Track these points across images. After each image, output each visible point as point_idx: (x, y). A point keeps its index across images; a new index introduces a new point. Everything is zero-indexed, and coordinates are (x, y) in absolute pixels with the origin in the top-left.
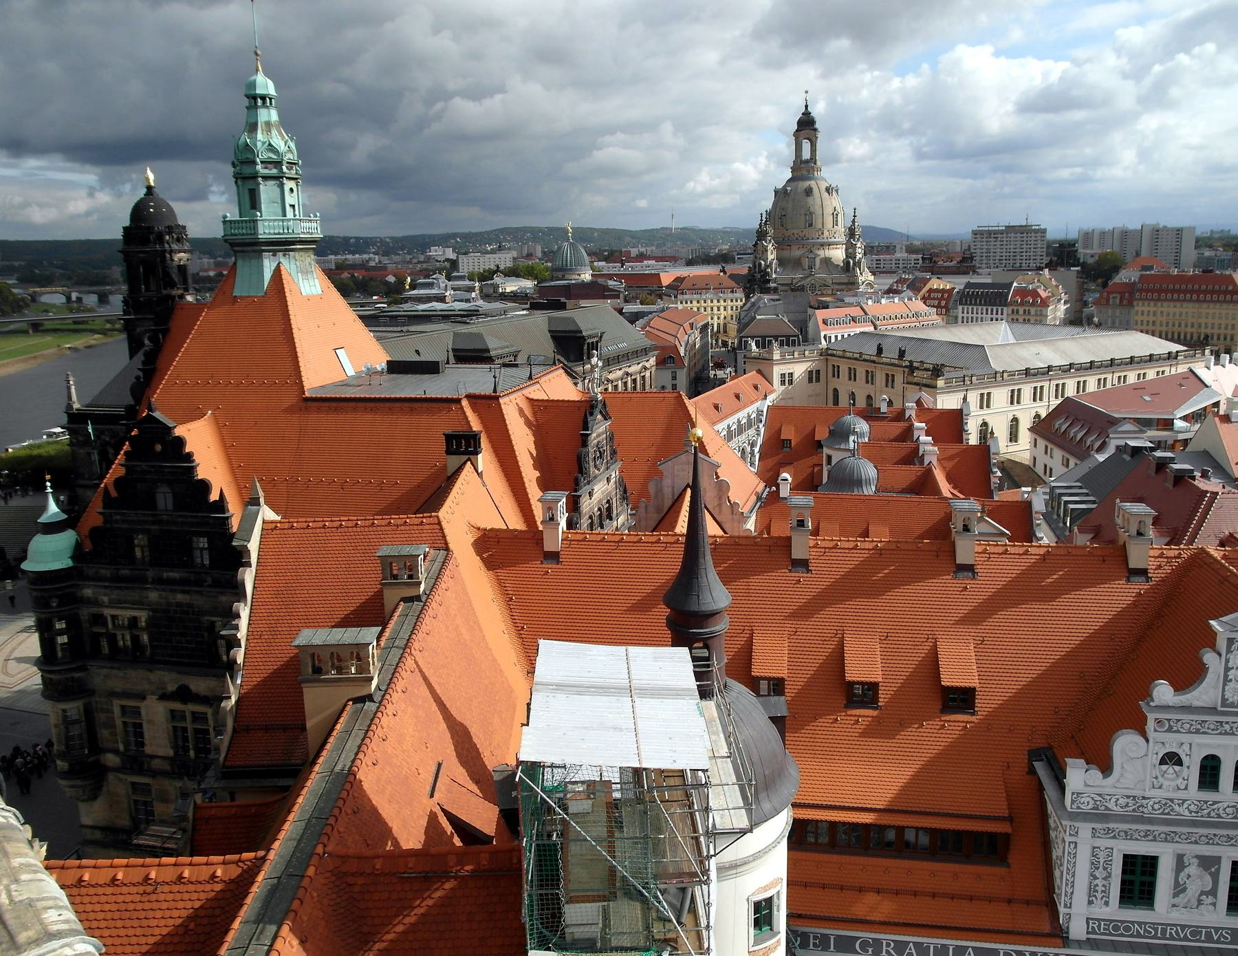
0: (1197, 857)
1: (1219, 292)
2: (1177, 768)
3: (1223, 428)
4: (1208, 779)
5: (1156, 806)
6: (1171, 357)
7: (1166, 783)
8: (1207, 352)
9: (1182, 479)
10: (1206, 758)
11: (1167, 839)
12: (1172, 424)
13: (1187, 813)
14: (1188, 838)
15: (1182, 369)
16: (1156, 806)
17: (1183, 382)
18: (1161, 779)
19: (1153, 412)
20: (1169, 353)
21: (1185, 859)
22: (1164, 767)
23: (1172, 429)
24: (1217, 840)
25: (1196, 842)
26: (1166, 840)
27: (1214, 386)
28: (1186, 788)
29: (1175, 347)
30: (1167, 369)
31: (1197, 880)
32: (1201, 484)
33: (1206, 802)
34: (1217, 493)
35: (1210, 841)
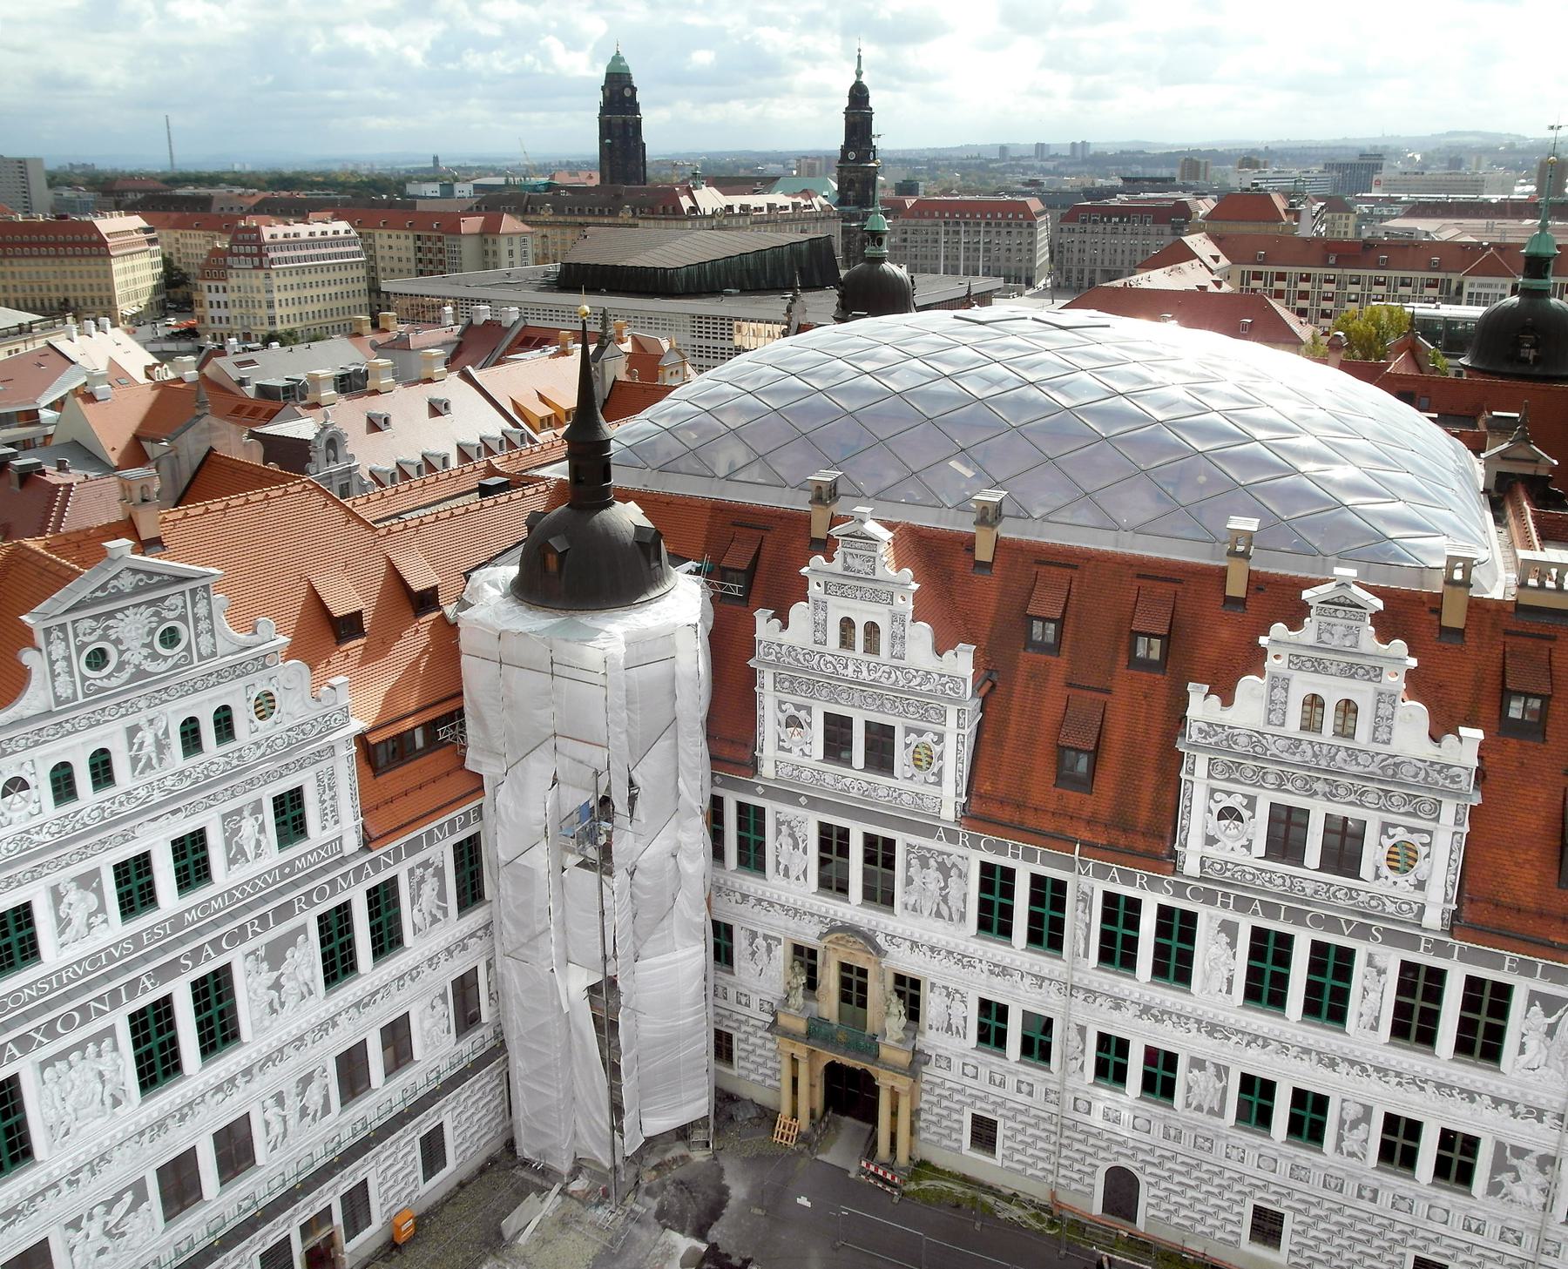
0: (73, 880)
1: (74, 244)
2: (23, 793)
3: (88, 409)
4: (64, 791)
5: (11, 847)
6: (22, 330)
7: (15, 816)
8: (69, 319)
9: (28, 476)
10: (55, 769)
11: (34, 875)
12: (38, 416)
13: (48, 838)
14: (59, 864)
15: (40, 344)
16: (11, 847)
17: (42, 360)
18: (8, 814)
19: (8, 405)
20: (20, 325)
21: (61, 888)
22: (9, 799)
23: (38, 423)
24: (90, 852)
25: (68, 865)
26: (33, 879)
27: (82, 361)
28: (40, 812)
29: (26, 317)
30: (21, 347)
31: (79, 903)
32: (53, 477)
33: (66, 816)
34: (71, 485)
35: (82, 856)
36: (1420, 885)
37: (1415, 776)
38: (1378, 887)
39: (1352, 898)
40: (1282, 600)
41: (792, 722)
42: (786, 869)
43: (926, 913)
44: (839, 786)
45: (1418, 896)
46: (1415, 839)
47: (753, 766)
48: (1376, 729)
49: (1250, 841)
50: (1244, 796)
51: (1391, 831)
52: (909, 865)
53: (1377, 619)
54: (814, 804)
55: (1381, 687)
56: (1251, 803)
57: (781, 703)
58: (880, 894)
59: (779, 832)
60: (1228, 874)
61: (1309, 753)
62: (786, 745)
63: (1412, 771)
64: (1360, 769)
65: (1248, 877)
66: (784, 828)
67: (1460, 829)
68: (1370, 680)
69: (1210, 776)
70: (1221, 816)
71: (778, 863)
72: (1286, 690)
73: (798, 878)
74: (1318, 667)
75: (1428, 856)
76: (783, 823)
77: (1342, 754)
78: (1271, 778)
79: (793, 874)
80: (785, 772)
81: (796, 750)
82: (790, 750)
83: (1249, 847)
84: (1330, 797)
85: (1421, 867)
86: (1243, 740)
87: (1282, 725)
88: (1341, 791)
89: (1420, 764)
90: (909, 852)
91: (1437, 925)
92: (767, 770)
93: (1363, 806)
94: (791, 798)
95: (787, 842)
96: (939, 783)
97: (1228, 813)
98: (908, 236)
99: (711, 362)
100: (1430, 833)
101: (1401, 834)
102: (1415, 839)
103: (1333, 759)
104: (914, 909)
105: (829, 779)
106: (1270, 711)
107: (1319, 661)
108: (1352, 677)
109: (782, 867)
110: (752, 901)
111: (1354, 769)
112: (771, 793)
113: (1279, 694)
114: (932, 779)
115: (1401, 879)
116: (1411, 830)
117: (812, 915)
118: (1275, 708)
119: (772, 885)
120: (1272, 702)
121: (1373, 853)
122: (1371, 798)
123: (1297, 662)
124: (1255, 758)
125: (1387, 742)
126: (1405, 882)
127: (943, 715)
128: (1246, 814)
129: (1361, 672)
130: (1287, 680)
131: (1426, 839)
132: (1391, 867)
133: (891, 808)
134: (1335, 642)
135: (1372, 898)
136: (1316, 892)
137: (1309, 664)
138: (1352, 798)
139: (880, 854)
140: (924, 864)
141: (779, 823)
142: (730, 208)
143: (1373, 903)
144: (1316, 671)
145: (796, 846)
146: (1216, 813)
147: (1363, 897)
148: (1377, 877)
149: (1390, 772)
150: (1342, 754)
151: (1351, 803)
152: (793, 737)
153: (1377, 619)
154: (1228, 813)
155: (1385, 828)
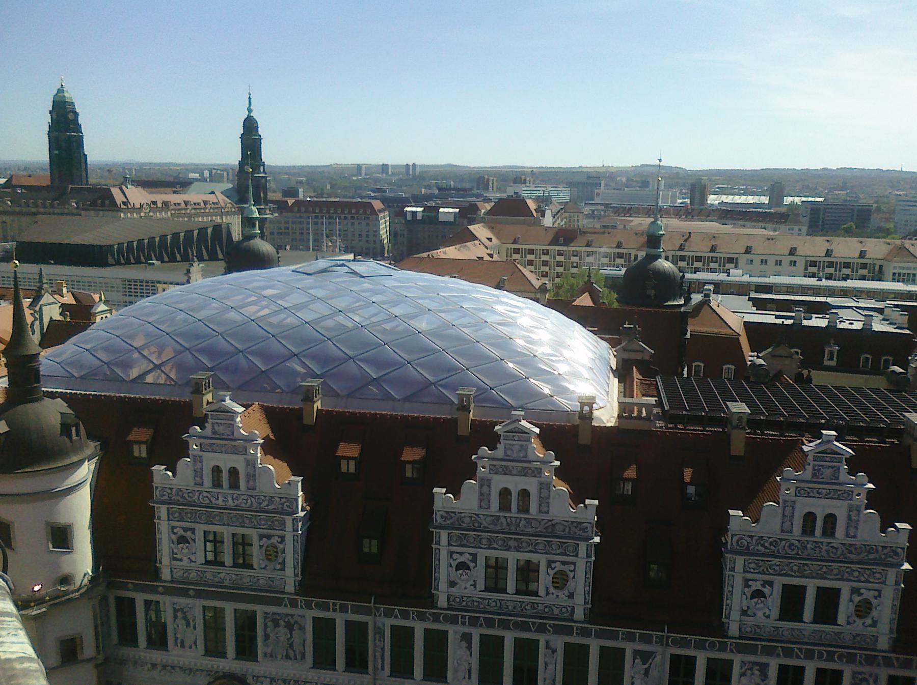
36: (571, 596)
38: (549, 600)
39: (535, 609)
40: (485, 434)
41: (182, 540)
42: (182, 642)
43: (279, 657)
45: (570, 603)
46: (566, 568)
47: (155, 574)
48: (540, 505)
49: (475, 581)
51: (553, 565)
52: (266, 626)
54: (199, 595)
56: (474, 557)
57: (173, 528)
58: (246, 650)
59: (175, 617)
60: (464, 603)
61: (505, 523)
62: (178, 556)
63: (562, 528)
64: (533, 530)
65: (476, 604)
66: (179, 614)
67: (589, 560)
68: (535, 476)
69: (449, 544)
71: (176, 639)
72: (489, 486)
73: (191, 647)
74: (506, 472)
75: (574, 577)
76: (179, 610)
77: (523, 522)
78: (484, 541)
79: (187, 644)
80: (178, 575)
81: (185, 559)
82: (181, 560)
83: (475, 586)
84: (518, 549)
85: (571, 584)
86: (467, 520)
87: (489, 508)
88: (524, 545)
89: (566, 524)
90: (265, 618)
91: (582, 618)
92: (166, 574)
93: (536, 552)
94: (184, 593)
95: (181, 622)
96: (283, 569)
97: (462, 566)
98: (290, 225)
99: (132, 299)
100: (574, 564)
101: (559, 567)
102: (566, 568)
103: (518, 525)
104: (271, 656)
105: (209, 576)
106: (481, 501)
107: (507, 467)
108: (525, 475)
109: (179, 641)
110: (159, 668)
111: (530, 530)
112: (168, 591)
113: (485, 489)
114: (278, 567)
115: (560, 593)
116: (564, 563)
117: (202, 671)
118: (484, 498)
119: (174, 655)
120: (482, 494)
121: (544, 579)
122: (541, 546)
123: (494, 470)
124: (474, 530)
125: (548, 512)
126: (562, 594)
127: (283, 523)
128: (472, 565)
129: (530, 472)
130: (489, 481)
131: (572, 567)
132: (555, 587)
134: (515, 455)
135: (546, 607)
136: (514, 608)
137: (501, 470)
138: (530, 548)
139: (246, 625)
140: (276, 624)
141: (175, 611)
142: (154, 203)
143: (547, 610)
144: (505, 474)
145: (188, 625)
146: (454, 566)
147: (541, 607)
148: (548, 594)
149: (550, 530)
150: (523, 522)
151: (530, 552)
152: (183, 551)
154: (462, 566)
155: (550, 563)
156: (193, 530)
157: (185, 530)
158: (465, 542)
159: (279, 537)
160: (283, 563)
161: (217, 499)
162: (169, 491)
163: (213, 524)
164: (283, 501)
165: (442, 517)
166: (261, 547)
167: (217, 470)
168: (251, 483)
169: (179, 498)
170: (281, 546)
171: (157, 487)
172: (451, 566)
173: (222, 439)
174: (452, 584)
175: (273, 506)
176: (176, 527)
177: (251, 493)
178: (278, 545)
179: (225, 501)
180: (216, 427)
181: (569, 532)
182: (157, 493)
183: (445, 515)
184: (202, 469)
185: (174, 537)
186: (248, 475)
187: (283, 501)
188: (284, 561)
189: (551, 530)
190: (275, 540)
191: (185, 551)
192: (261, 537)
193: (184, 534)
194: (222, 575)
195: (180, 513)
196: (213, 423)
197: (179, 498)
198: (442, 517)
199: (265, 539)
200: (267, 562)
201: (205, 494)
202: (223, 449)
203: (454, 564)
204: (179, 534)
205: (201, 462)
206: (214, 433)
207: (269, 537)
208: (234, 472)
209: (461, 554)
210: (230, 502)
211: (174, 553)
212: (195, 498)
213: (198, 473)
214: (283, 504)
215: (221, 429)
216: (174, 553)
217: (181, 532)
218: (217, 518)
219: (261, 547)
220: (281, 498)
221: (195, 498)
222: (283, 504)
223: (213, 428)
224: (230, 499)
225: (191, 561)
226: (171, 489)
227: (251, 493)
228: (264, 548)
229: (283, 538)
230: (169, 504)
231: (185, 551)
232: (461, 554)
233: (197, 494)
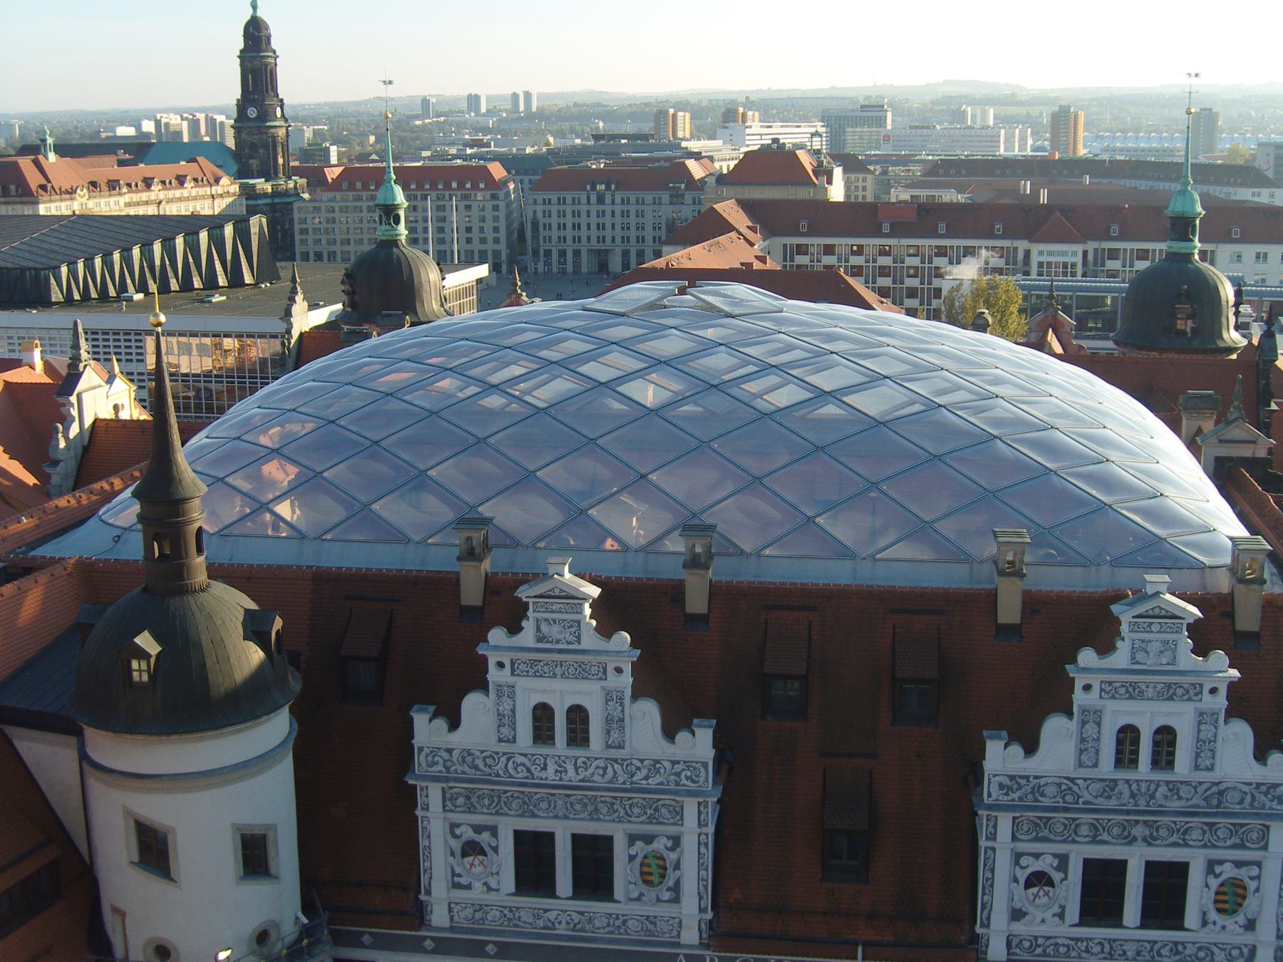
36: (1250, 925)
37: (1241, 802)
38: (1205, 936)
39: (1178, 953)
40: (1092, 621)
41: (472, 849)
44: (541, 923)
45: (1248, 938)
46: (1243, 873)
47: (418, 915)
48: (1198, 756)
49: (1063, 908)
50: (1055, 856)
51: (1218, 869)
53: (1195, 629)
55: (1202, 706)
56: (1063, 862)
57: (454, 826)
60: (1039, 950)
61: (1126, 792)
62: (463, 881)
63: (1238, 796)
64: (1183, 803)
65: (1062, 950)
68: (1190, 699)
69: (1014, 838)
70: (1029, 884)
72: (1099, 724)
74: (1133, 692)
75: (1257, 890)
77: (1163, 789)
78: (1084, 830)
80: (463, 916)
81: (478, 885)
82: (469, 887)
83: (1061, 915)
84: (1149, 841)
85: (1251, 903)
86: (1050, 790)
87: (1096, 765)
88: (1163, 832)
89: (1246, 788)
92: (439, 917)
93: (1186, 845)
96: (676, 900)
97: (1038, 879)
100: (1259, 864)
101: (1228, 871)
102: (1243, 873)
103: (1152, 796)
105: (526, 916)
106: (1081, 752)
107: (1134, 685)
108: (1171, 698)
111: (1175, 805)
113: (1090, 729)
114: (667, 895)
115: (1229, 922)
116: (1239, 864)
118: (1086, 749)
120: (1083, 740)
121: (1198, 896)
122: (1195, 834)
123: (1110, 692)
124: (1066, 810)
125: (1211, 768)
126: (1233, 924)
128: (1057, 876)
129: (1180, 691)
130: (1098, 713)
131: (1254, 871)
132: (1219, 911)
133: (611, 941)
134: (1150, 662)
135: (1200, 949)
136: (1138, 953)
137: (1122, 690)
138: (1175, 838)
144: (1131, 698)
146: (1022, 880)
147: (1190, 950)
148: (1204, 923)
149: (1215, 802)
150: (1163, 789)
151: (1175, 844)
153: (1195, 629)
154: (1038, 879)
155: (1211, 866)
156: (494, 830)
157: (478, 829)
158: (1045, 833)
159: (669, 838)
160: (676, 888)
161: (545, 768)
162: (446, 756)
163: (534, 815)
164: (678, 768)
165: (1001, 786)
166: (632, 858)
167: (543, 714)
168: (615, 735)
169: (466, 769)
170: (673, 856)
171: (421, 749)
172: (1016, 880)
173: (560, 651)
174: (1017, 915)
175: (658, 779)
176: (458, 825)
177: (613, 753)
178: (666, 854)
179: (561, 771)
180: (544, 628)
181: (1251, 805)
182: (420, 761)
183: (1007, 781)
184: (513, 711)
185: (456, 845)
186: (608, 720)
187: (678, 768)
188: (678, 883)
189: (1216, 799)
190: (660, 845)
191: (478, 869)
192: (632, 838)
193: (476, 837)
194: (552, 915)
195: (468, 798)
196: (538, 620)
197: (466, 769)
198: (1001, 786)
199: (639, 844)
200: (644, 888)
201: (520, 759)
202: (558, 671)
203: (1022, 876)
204: (464, 839)
205: (512, 696)
206: (540, 640)
207: (648, 839)
208: (578, 716)
209: (1037, 856)
210: (571, 772)
211: (454, 874)
212: (499, 768)
213: (506, 720)
214: (678, 774)
215: (554, 631)
216: (454, 874)
217: (469, 834)
218: (544, 805)
219: (632, 858)
220: (674, 763)
221: (499, 768)
222: (678, 774)
223: (538, 629)
224: (570, 767)
225: (490, 889)
226: (450, 751)
227: (613, 753)
228: (639, 860)
229: (676, 841)
230: (447, 780)
231: (478, 869)
232: (1037, 856)
233: (504, 759)
